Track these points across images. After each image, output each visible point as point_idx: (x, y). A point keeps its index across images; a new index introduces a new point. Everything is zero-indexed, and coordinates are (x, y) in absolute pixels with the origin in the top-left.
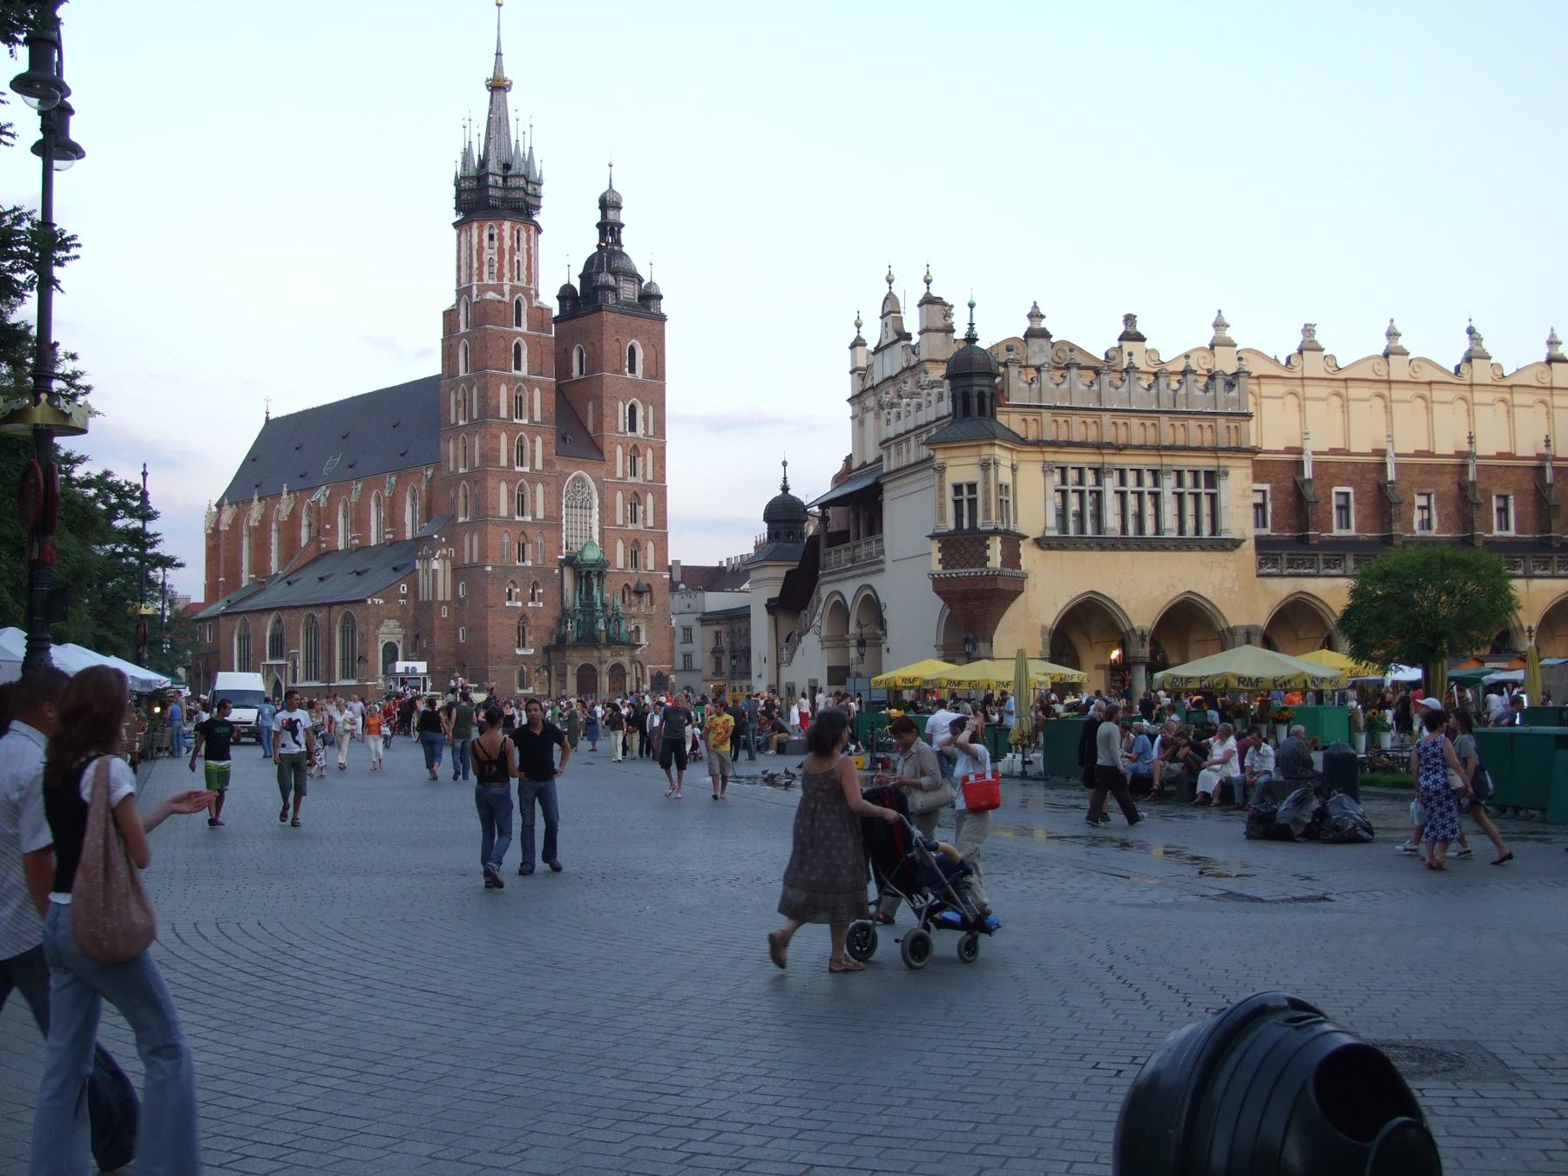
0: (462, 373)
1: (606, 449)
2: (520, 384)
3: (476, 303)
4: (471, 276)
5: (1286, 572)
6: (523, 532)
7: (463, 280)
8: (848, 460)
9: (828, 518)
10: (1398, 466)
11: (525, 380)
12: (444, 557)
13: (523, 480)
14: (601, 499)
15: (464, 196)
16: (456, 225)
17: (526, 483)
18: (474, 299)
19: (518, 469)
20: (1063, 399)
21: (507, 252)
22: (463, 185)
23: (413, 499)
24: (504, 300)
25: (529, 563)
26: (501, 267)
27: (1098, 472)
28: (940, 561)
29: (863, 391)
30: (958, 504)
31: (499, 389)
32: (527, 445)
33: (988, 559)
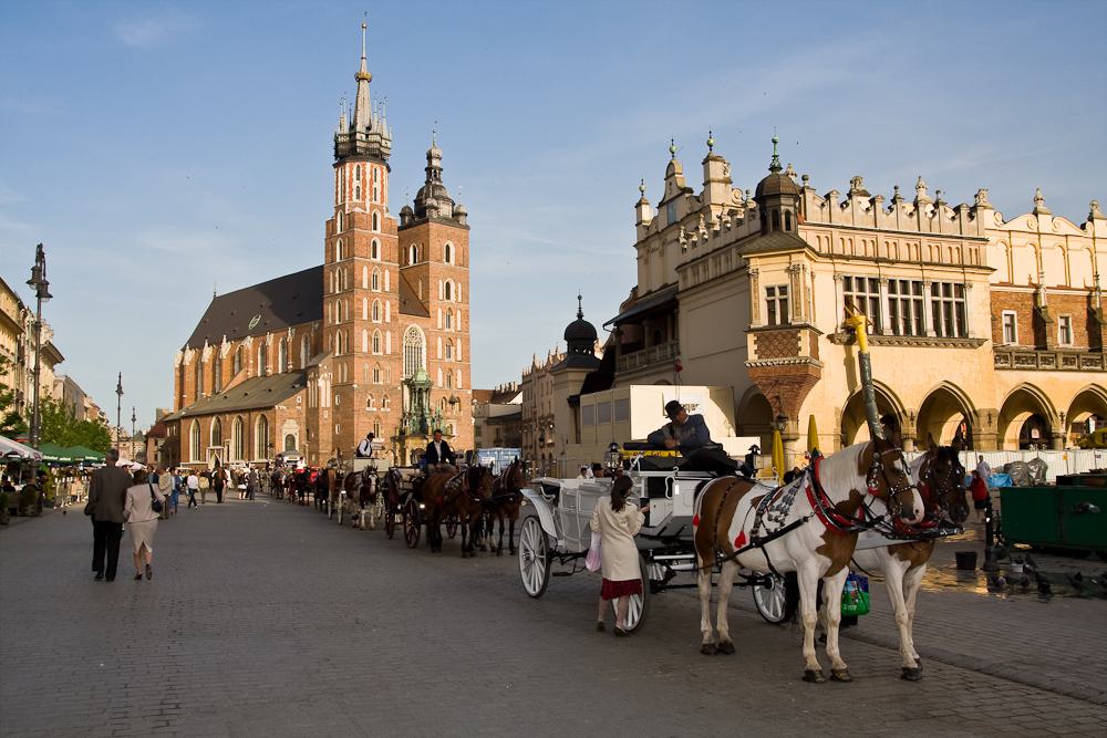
0: (338, 260)
1: (431, 310)
5: (1014, 367)
7: (339, 200)
8: (635, 290)
9: (622, 333)
10: (1049, 297)
14: (427, 341)
16: (335, 166)
18: (347, 212)
19: (374, 322)
20: (848, 221)
21: (368, 182)
23: (306, 343)
25: (381, 383)
26: (364, 191)
27: (875, 283)
28: (756, 352)
29: (647, 239)
30: (771, 304)
32: (380, 306)
33: (800, 349)
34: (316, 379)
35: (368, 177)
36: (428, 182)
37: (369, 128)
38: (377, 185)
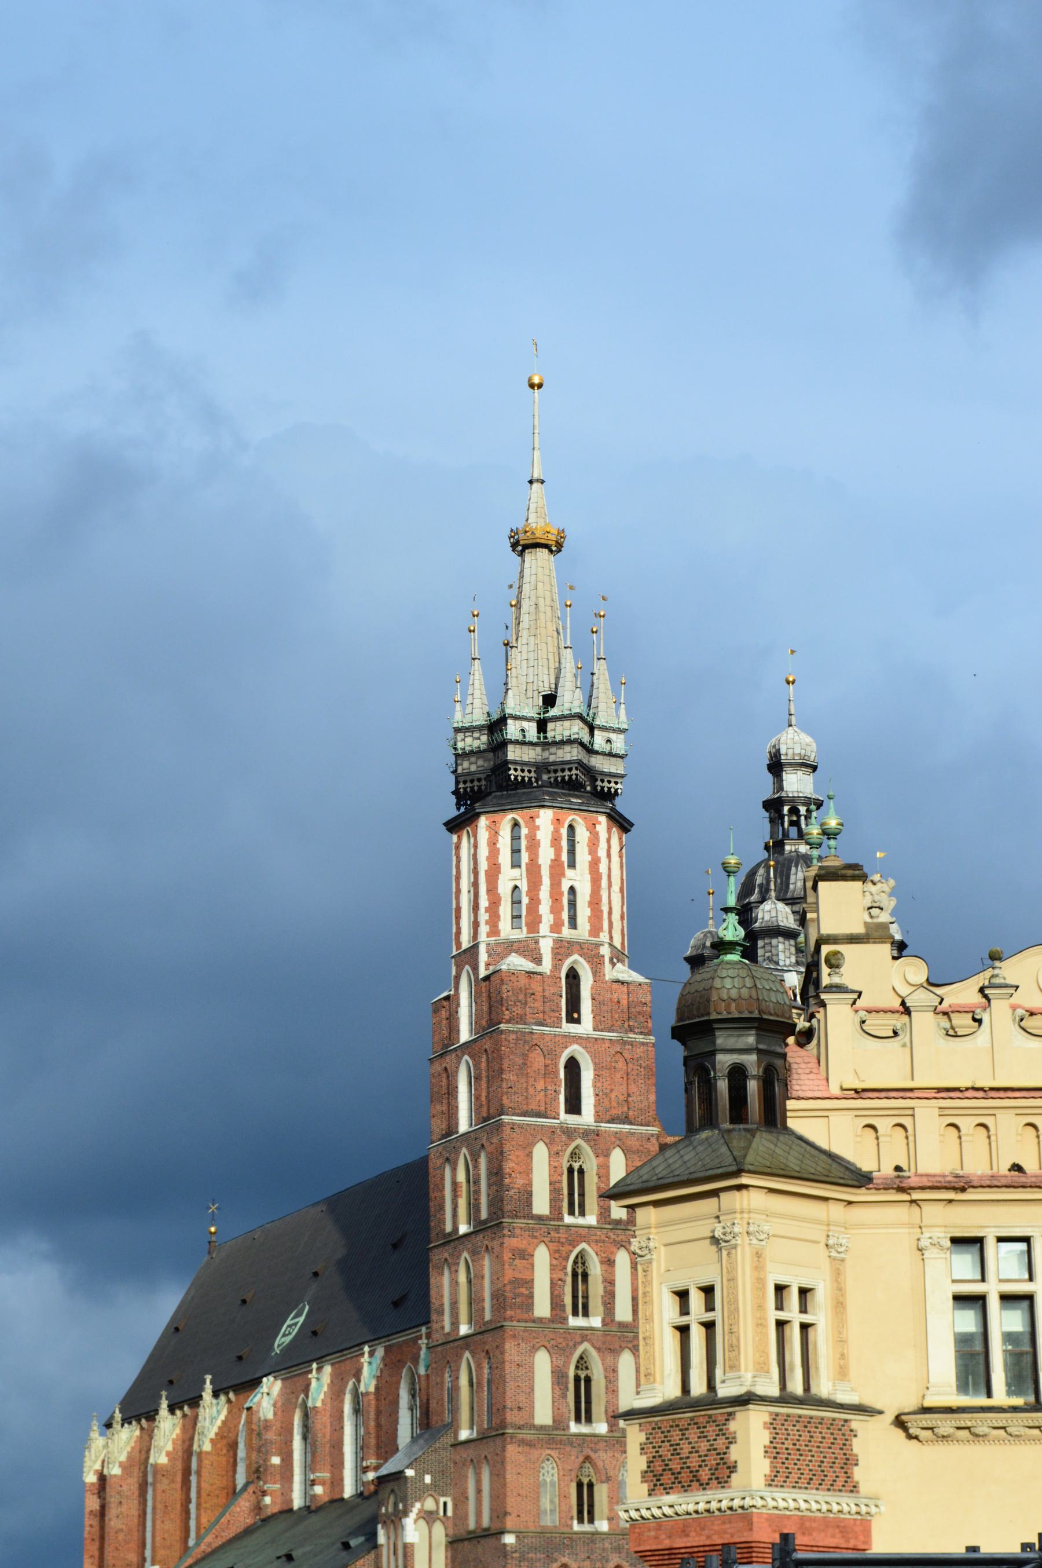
2: (579, 1141)
3: (487, 978)
4: (476, 925)
6: (587, 1458)
11: (591, 1135)
12: (429, 1517)
13: (586, 1345)
15: (465, 765)
17: (593, 1353)
19: (574, 1322)
22: (460, 745)
24: (539, 969)
25: (602, 1525)
26: (534, 902)
31: (530, 1155)
32: (595, 1269)
34: (395, 1520)
35: (546, 855)
36: (776, 846)
37: (550, 700)
38: (579, 878)
